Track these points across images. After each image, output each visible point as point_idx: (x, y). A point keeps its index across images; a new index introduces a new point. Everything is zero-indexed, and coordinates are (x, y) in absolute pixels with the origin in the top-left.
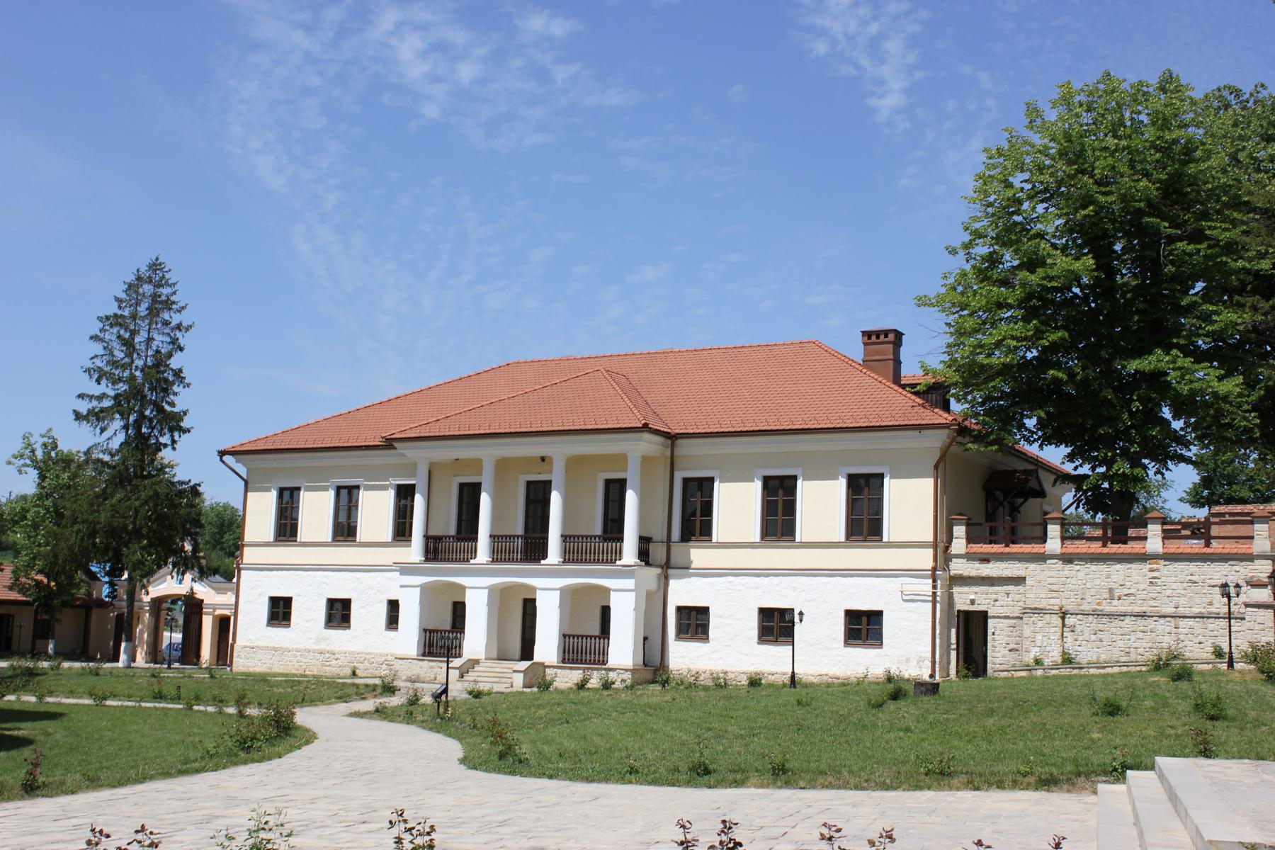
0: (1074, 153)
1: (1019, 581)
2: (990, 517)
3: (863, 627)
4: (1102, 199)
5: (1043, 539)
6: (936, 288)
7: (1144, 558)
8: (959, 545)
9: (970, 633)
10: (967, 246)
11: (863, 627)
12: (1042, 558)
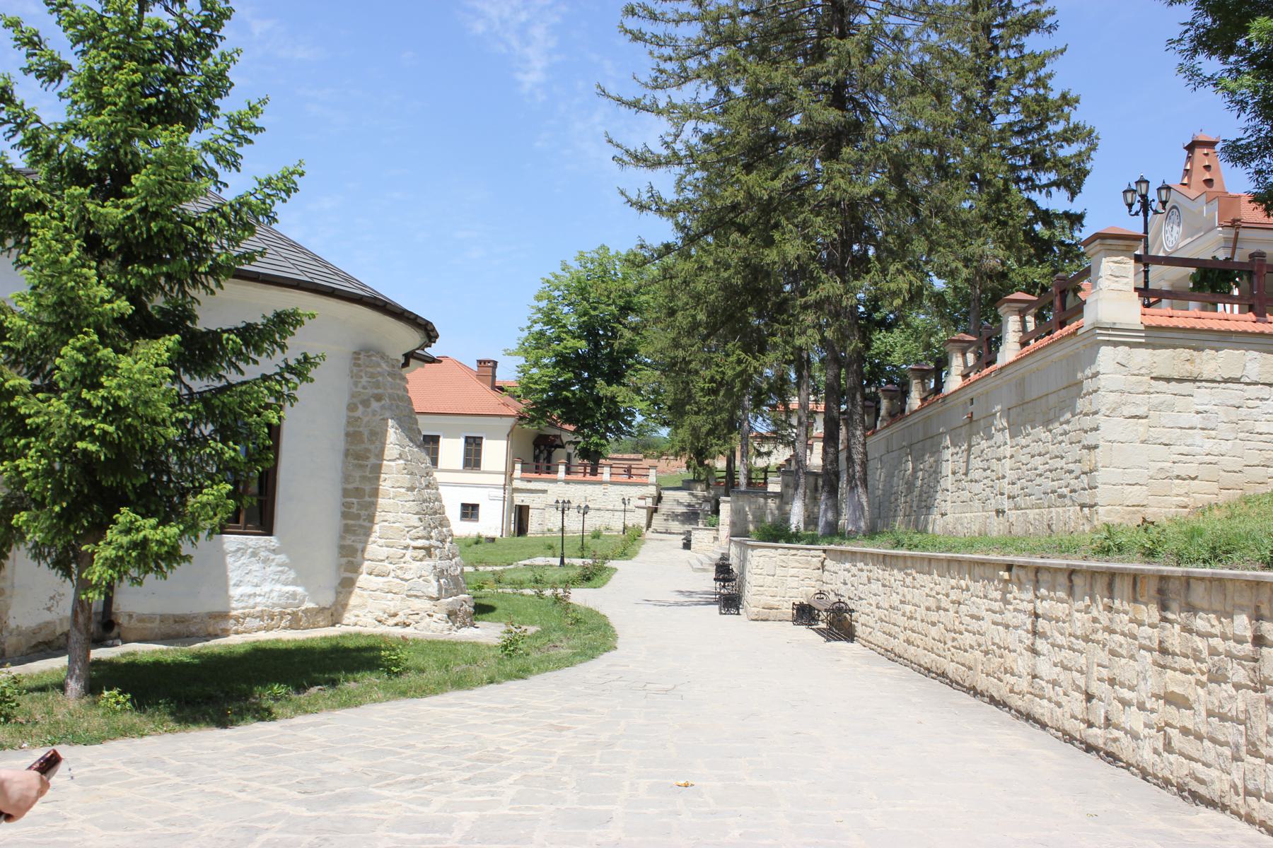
0: (583, 291)
1: (545, 491)
2: (536, 458)
3: (470, 511)
4: (593, 313)
5: (557, 472)
6: (514, 346)
7: (601, 483)
8: (518, 473)
9: (521, 515)
10: (529, 328)
11: (470, 511)
12: (556, 481)
